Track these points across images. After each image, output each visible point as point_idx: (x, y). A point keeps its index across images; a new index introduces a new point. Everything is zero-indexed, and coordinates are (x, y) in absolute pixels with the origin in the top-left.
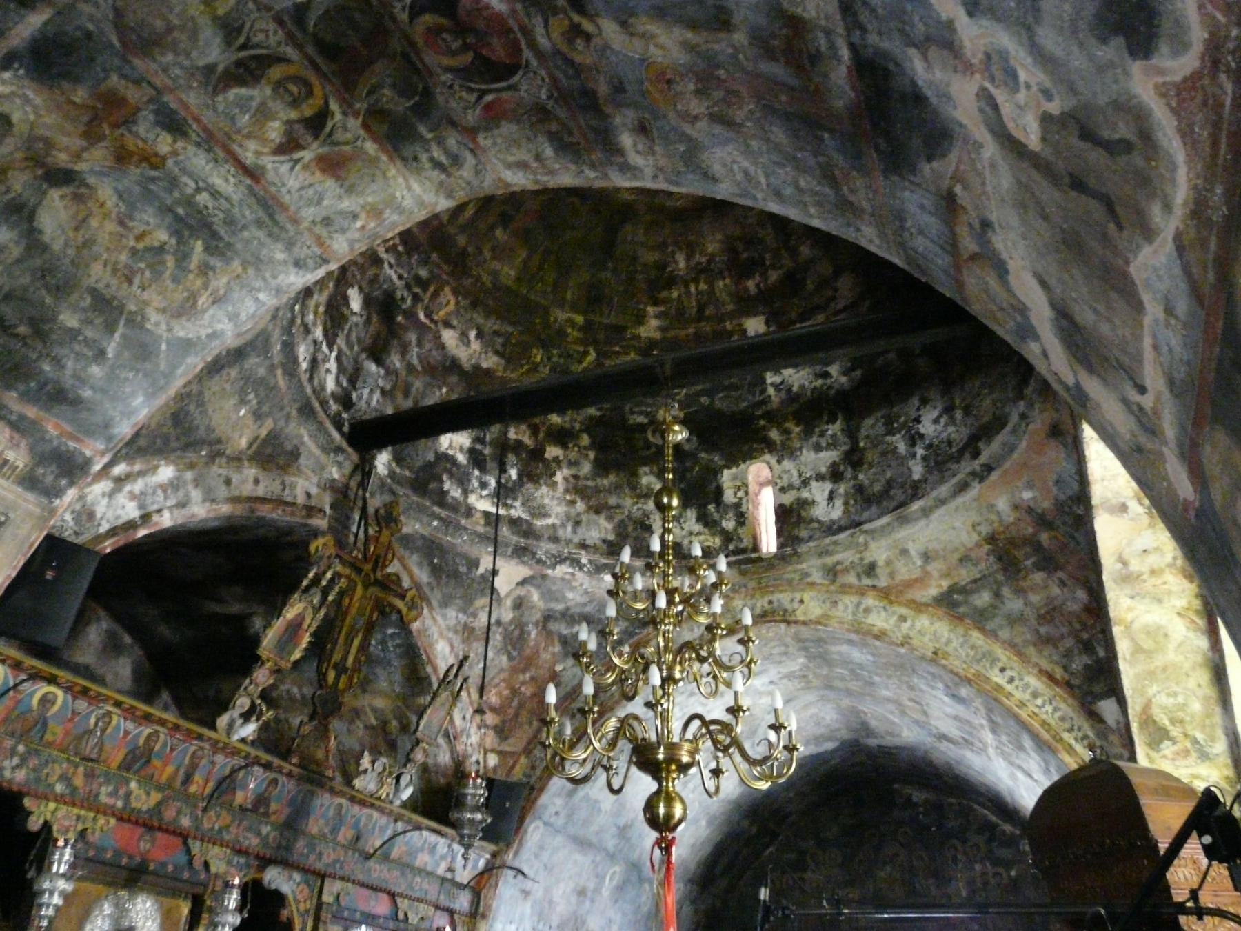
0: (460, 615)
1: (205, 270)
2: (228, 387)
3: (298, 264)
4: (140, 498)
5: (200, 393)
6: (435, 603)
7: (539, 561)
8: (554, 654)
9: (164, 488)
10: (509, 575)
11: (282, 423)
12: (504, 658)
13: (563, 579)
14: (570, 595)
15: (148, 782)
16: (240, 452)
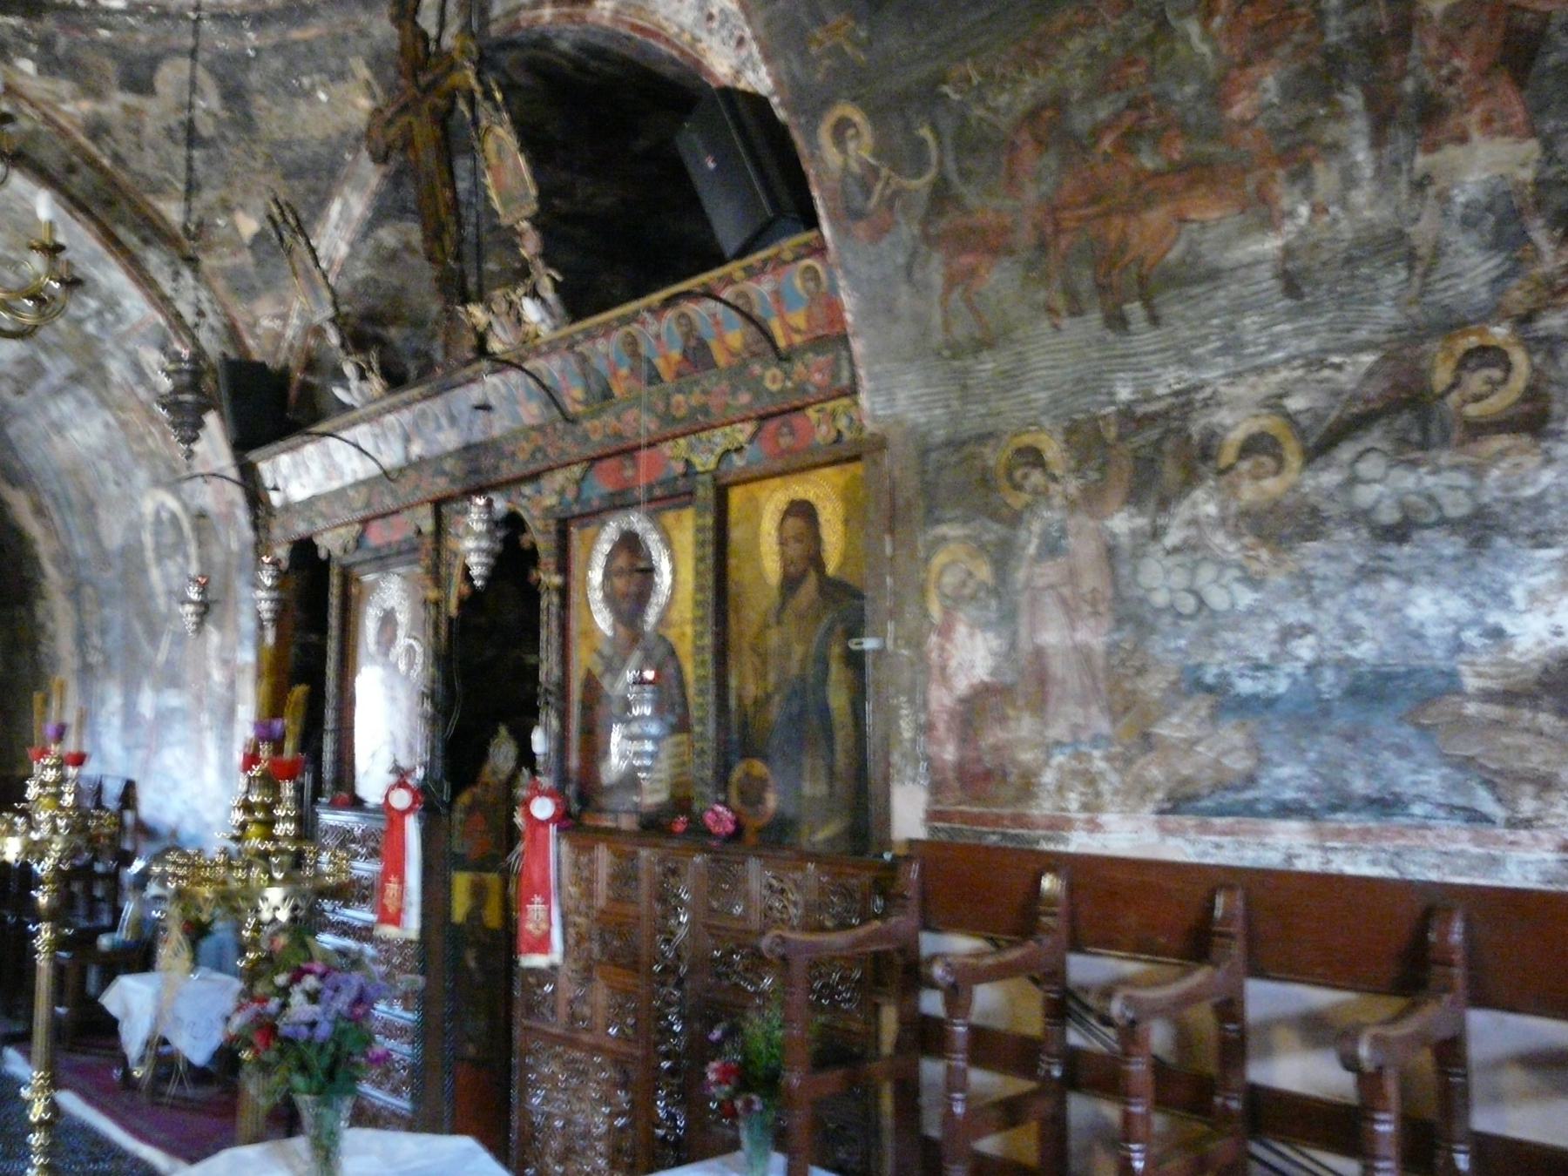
2: (278, 110)
5: (275, 144)
11: (364, 45)
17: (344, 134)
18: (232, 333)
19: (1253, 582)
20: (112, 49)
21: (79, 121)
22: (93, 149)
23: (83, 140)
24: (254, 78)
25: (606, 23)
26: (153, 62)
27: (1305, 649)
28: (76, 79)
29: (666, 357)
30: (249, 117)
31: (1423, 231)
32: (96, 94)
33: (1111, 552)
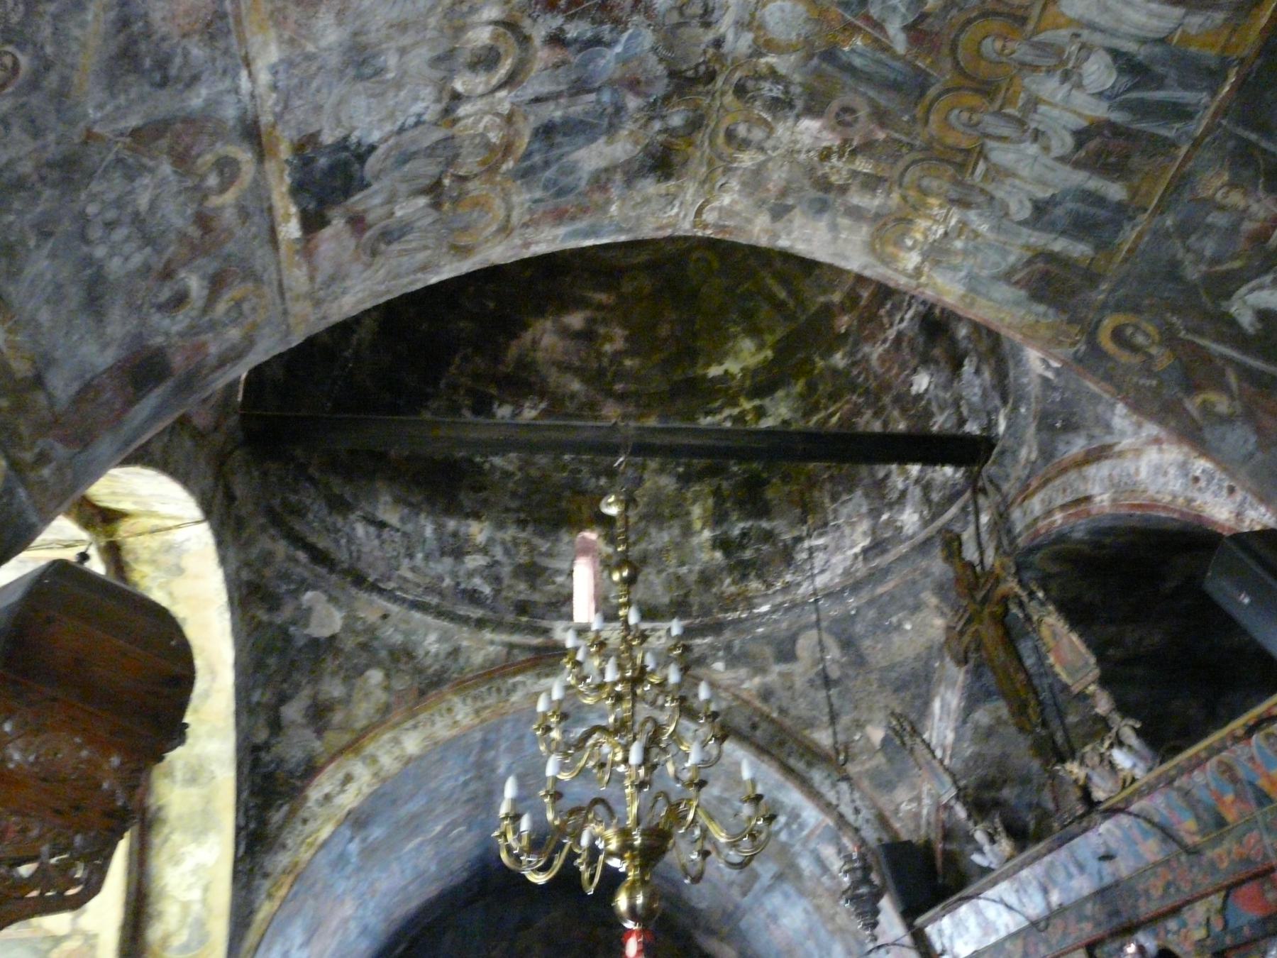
2: (880, 646)
5: (883, 669)
17: (931, 647)
18: (883, 821)
20: (766, 638)
21: (754, 692)
22: (765, 708)
24: (859, 628)
25: (1107, 510)
26: (793, 639)
28: (747, 664)
32: (762, 670)
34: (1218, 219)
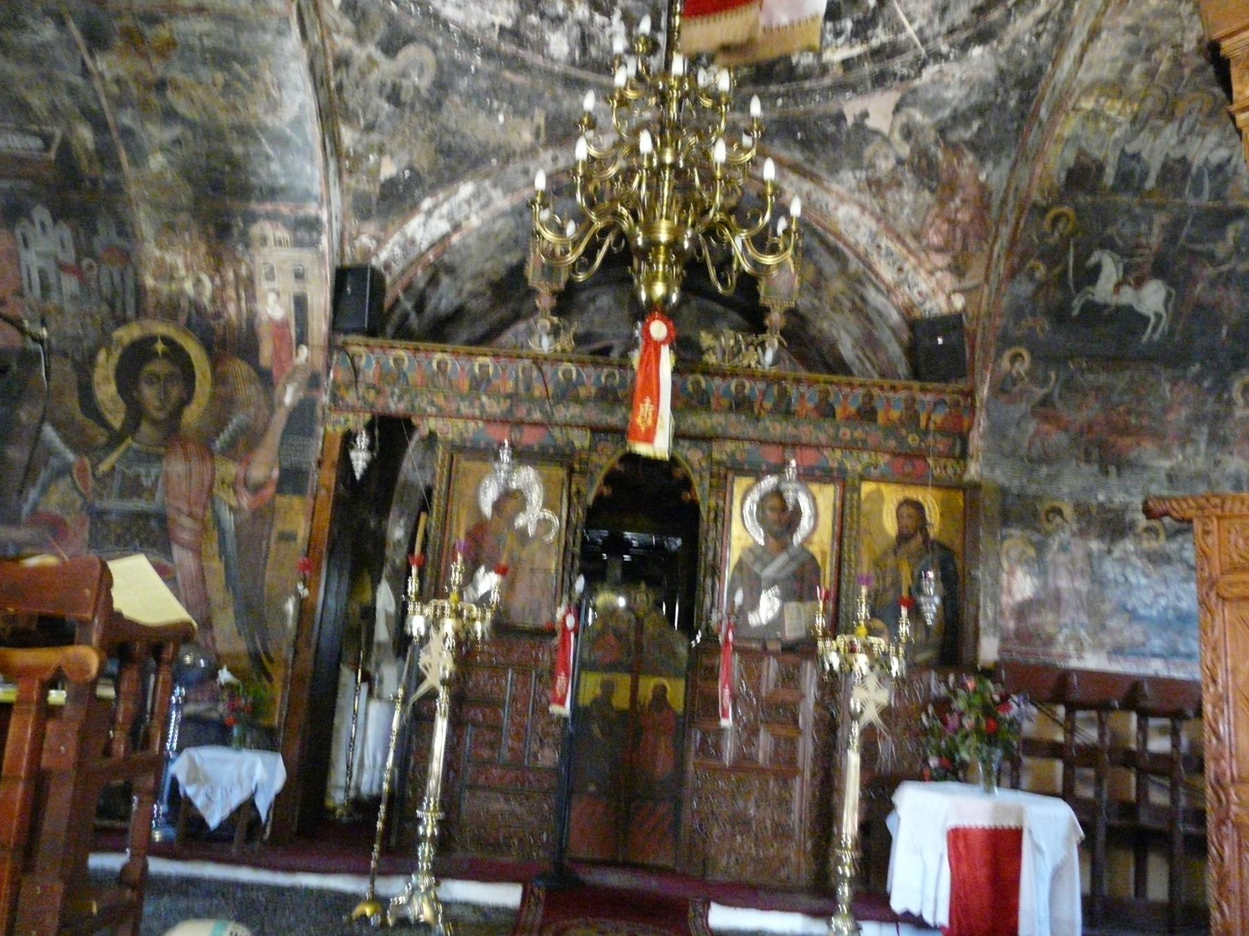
0: (858, 174)
1: (255, 76)
2: (463, 109)
3: (280, 33)
4: (450, 217)
5: (446, 129)
6: (823, 174)
7: (902, 79)
8: (971, 166)
9: (468, 202)
10: (877, 109)
12: (926, 194)
13: (933, 82)
14: (949, 94)
15: (494, 395)
16: (532, 145)
19: (1147, 576)
23: (331, 63)
24: (463, 83)
26: (409, 40)
27: (1163, 602)
28: (357, 23)
29: (845, 409)
30: (439, 104)
31: (1215, 475)
32: (360, 39)
33: (1089, 555)
34: (1144, 228)
